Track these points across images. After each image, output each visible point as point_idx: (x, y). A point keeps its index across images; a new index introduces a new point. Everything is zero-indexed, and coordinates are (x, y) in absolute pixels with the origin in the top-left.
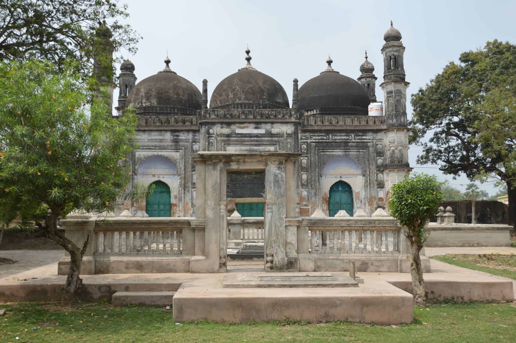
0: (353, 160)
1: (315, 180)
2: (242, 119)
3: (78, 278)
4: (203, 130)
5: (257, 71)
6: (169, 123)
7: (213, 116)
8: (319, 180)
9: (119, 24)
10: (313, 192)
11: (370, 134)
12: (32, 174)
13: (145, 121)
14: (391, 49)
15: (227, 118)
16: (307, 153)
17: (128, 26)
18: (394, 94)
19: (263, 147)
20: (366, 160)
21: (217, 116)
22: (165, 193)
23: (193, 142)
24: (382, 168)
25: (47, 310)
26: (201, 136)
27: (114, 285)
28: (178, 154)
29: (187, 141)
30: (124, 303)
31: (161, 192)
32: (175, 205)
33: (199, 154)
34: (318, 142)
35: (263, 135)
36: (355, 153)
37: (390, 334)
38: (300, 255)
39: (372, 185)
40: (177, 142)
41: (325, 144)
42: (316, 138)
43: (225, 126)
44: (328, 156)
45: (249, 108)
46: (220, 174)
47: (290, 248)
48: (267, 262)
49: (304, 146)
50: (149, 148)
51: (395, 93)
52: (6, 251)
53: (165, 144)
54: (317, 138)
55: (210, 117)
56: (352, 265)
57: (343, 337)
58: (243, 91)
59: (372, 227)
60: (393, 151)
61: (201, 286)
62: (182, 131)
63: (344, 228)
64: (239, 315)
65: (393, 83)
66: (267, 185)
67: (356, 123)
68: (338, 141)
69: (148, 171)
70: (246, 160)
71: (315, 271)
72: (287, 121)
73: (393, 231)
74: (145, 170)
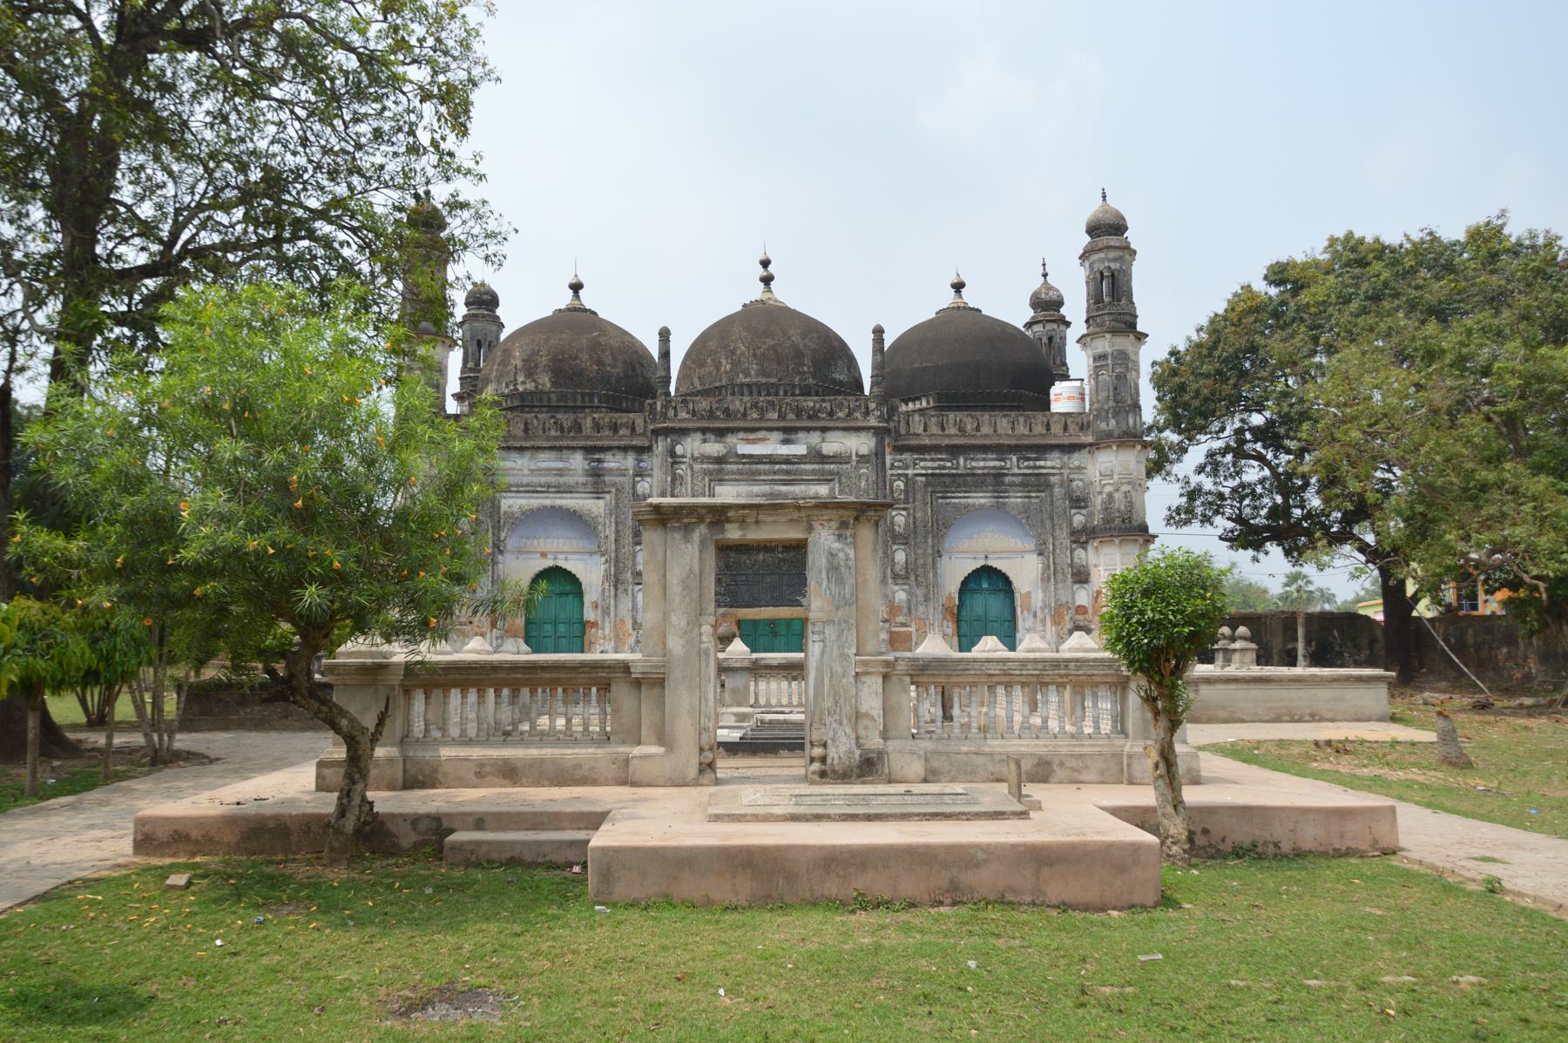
0: (1014, 517)
1: (924, 565)
3: (364, 798)
4: (661, 446)
5: (787, 308)
7: (683, 415)
8: (934, 563)
9: (461, 199)
10: (920, 592)
11: (1056, 454)
12: (256, 552)
14: (1102, 255)
15: (717, 418)
16: (906, 501)
17: (484, 202)
19: (803, 487)
20: (1046, 516)
21: (694, 413)
23: (635, 475)
24: (1083, 537)
25: (291, 876)
26: (655, 462)
27: (448, 815)
29: (622, 472)
30: (475, 858)
31: (561, 594)
32: (594, 624)
33: (651, 505)
35: (801, 459)
37: (1106, 933)
38: (889, 743)
39: (1060, 576)
41: (947, 480)
42: (927, 465)
44: (956, 506)
45: (769, 394)
46: (701, 551)
47: (866, 728)
48: (812, 760)
49: (900, 484)
50: (532, 490)
51: (1114, 358)
52: (194, 735)
53: (571, 480)
54: (929, 464)
56: (1013, 766)
57: (992, 940)
58: (755, 355)
59: (1061, 676)
60: (1110, 495)
61: (655, 818)
62: (609, 449)
63: (995, 679)
64: (746, 886)
65: (1108, 336)
66: (811, 576)
67: (1021, 429)
70: (761, 517)
71: (925, 781)
72: (859, 424)
73: (1111, 685)
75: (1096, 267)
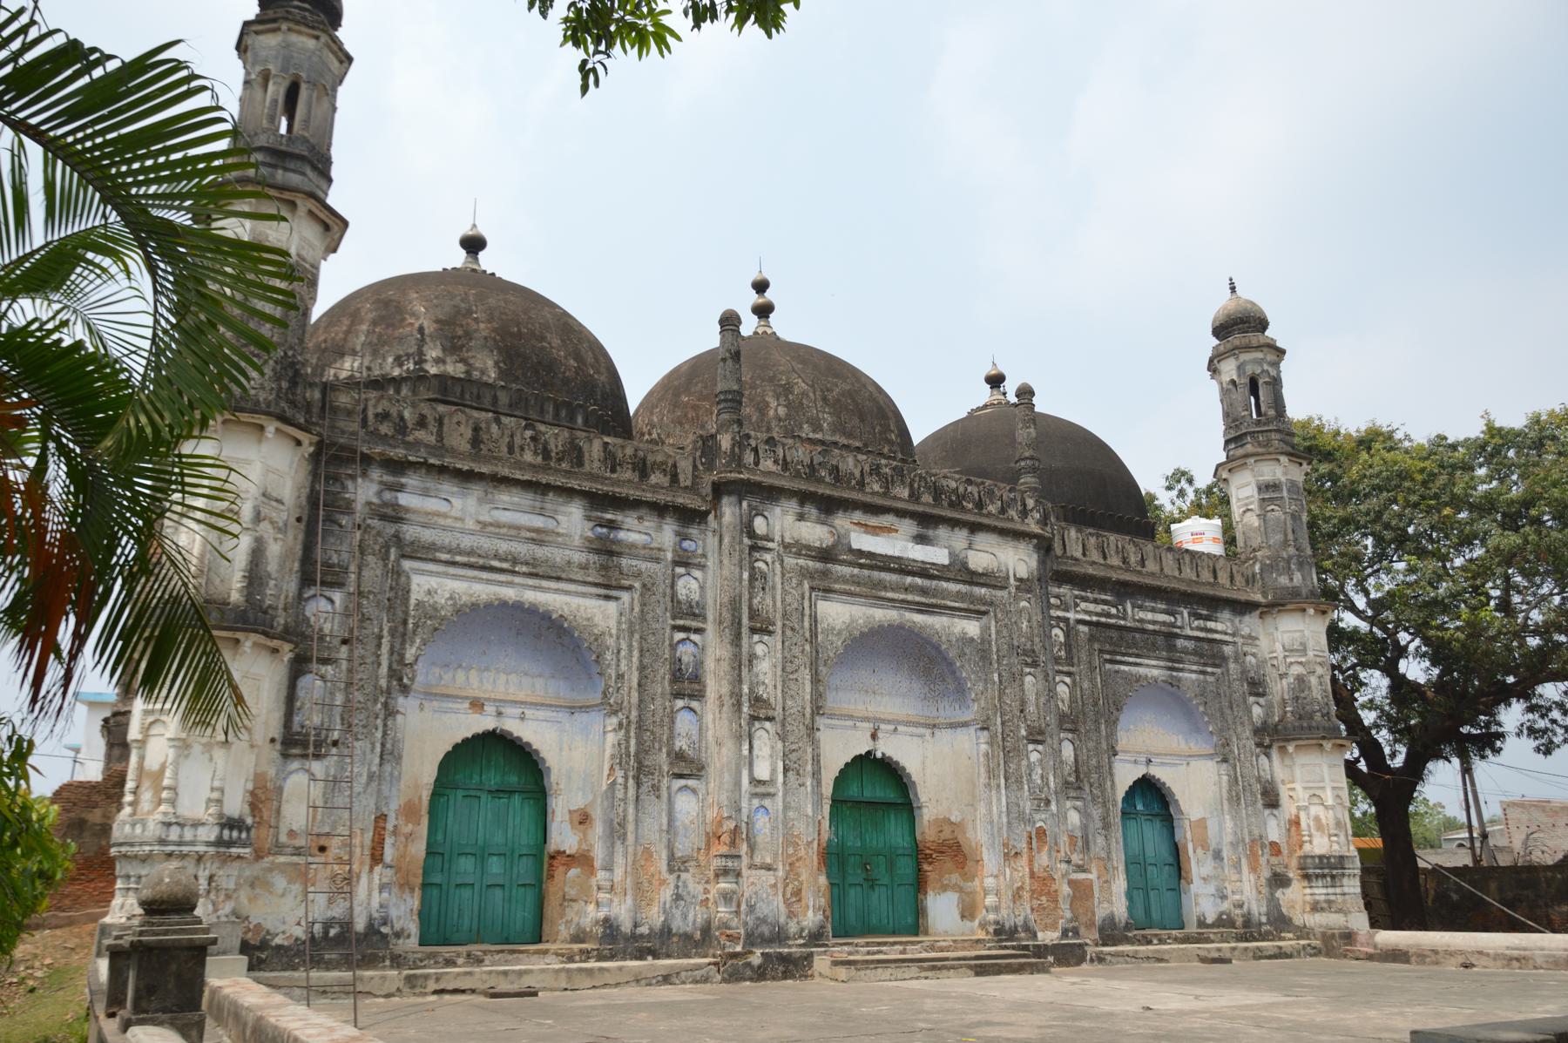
1: (1099, 767)
2: (874, 493)
4: (729, 511)
6: (580, 464)
7: (767, 464)
11: (1226, 614)
13: (469, 434)
14: (1259, 355)
15: (820, 480)
18: (1285, 494)
21: (785, 465)
22: (517, 798)
28: (612, 607)
31: (497, 792)
32: (582, 860)
34: (1098, 624)
36: (1194, 676)
40: (611, 553)
41: (1114, 634)
43: (814, 512)
50: (482, 565)
54: (1092, 607)
55: (757, 463)
58: (825, 399)
60: (1300, 679)
62: (635, 504)
65: (1284, 459)
68: (1151, 627)
69: (447, 677)
74: (437, 670)
75: (1249, 369)
